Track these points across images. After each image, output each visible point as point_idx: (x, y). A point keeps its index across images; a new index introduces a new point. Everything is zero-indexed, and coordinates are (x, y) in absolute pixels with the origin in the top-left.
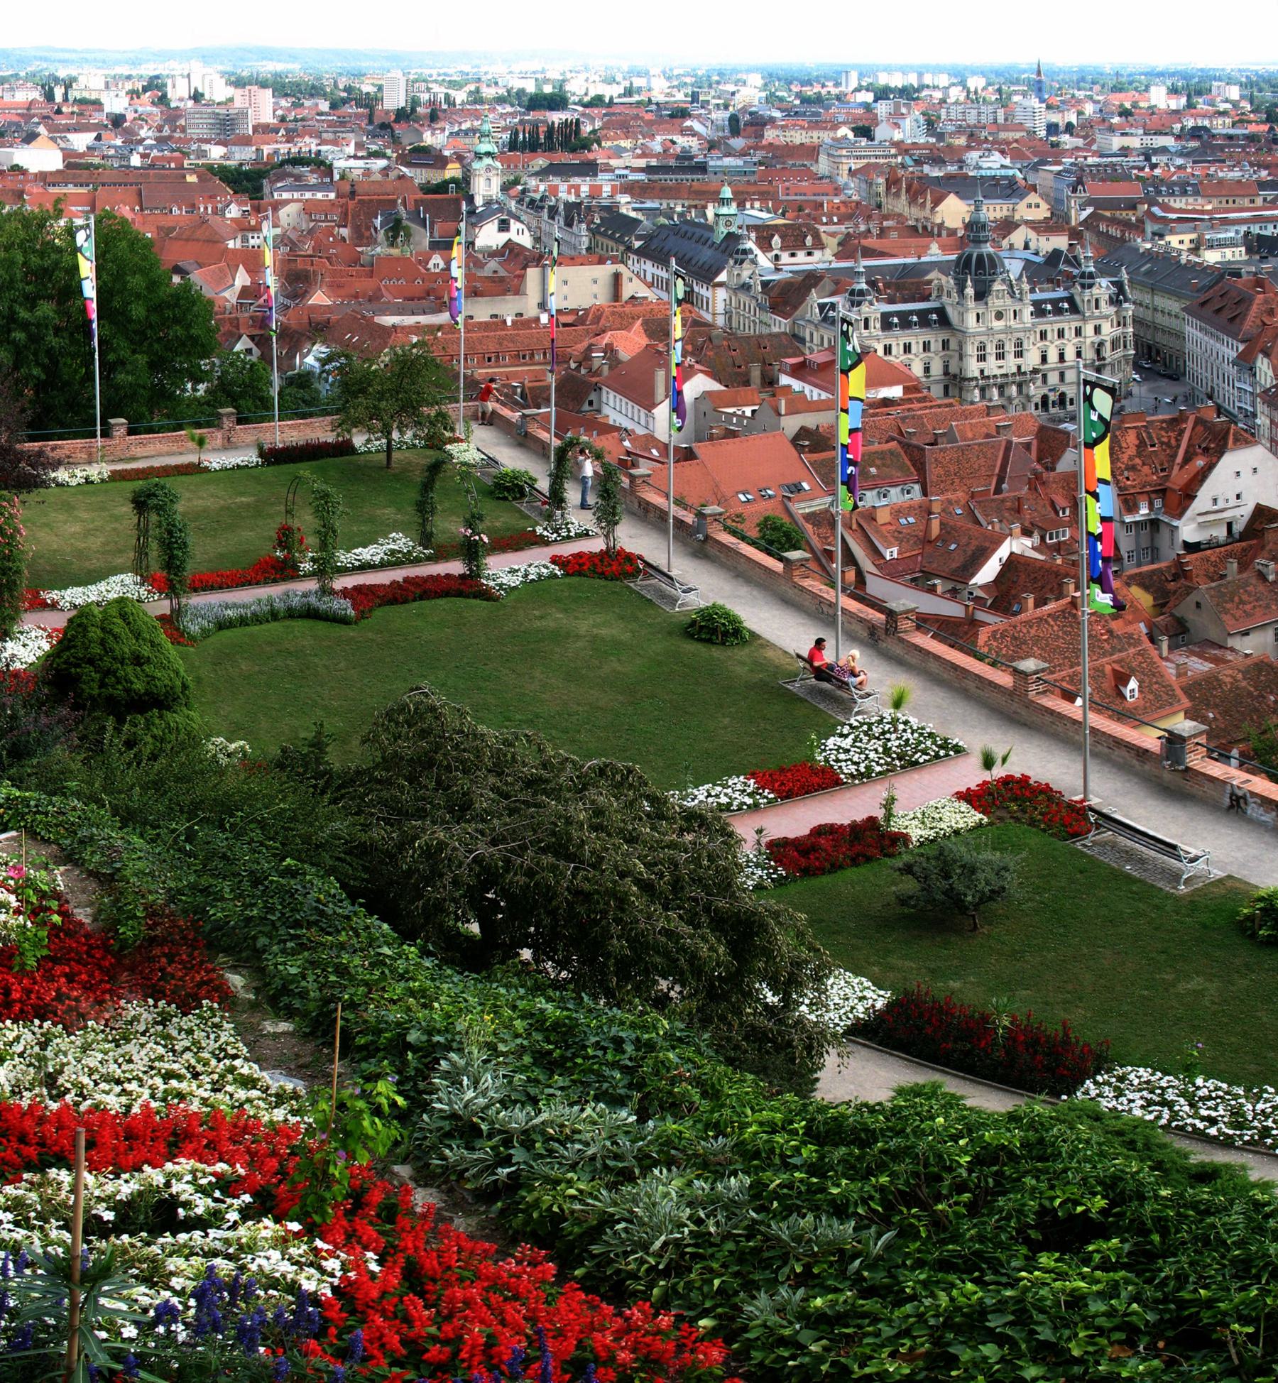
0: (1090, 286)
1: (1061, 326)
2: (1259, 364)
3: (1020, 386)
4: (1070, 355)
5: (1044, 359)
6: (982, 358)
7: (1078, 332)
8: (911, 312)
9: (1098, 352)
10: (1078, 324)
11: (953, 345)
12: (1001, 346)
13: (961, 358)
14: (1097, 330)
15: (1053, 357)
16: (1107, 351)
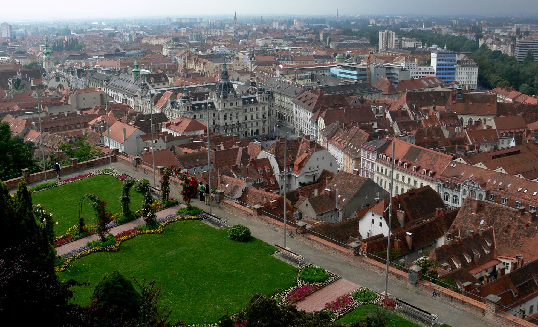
1: (251, 107)
2: (319, 120)
3: (238, 128)
4: (255, 117)
5: (246, 119)
6: (226, 119)
8: (202, 104)
9: (264, 116)
10: (257, 106)
11: (216, 115)
12: (232, 115)
13: (219, 119)
14: (263, 108)
15: (249, 118)
16: (266, 116)
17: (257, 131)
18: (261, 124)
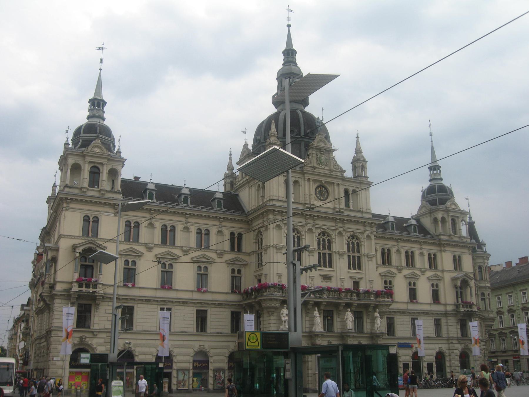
0: (443, 202)
3: (358, 318)
7: (433, 262)
11: (248, 244)
12: (325, 241)
14: (457, 262)
17: (440, 356)
18: (451, 328)
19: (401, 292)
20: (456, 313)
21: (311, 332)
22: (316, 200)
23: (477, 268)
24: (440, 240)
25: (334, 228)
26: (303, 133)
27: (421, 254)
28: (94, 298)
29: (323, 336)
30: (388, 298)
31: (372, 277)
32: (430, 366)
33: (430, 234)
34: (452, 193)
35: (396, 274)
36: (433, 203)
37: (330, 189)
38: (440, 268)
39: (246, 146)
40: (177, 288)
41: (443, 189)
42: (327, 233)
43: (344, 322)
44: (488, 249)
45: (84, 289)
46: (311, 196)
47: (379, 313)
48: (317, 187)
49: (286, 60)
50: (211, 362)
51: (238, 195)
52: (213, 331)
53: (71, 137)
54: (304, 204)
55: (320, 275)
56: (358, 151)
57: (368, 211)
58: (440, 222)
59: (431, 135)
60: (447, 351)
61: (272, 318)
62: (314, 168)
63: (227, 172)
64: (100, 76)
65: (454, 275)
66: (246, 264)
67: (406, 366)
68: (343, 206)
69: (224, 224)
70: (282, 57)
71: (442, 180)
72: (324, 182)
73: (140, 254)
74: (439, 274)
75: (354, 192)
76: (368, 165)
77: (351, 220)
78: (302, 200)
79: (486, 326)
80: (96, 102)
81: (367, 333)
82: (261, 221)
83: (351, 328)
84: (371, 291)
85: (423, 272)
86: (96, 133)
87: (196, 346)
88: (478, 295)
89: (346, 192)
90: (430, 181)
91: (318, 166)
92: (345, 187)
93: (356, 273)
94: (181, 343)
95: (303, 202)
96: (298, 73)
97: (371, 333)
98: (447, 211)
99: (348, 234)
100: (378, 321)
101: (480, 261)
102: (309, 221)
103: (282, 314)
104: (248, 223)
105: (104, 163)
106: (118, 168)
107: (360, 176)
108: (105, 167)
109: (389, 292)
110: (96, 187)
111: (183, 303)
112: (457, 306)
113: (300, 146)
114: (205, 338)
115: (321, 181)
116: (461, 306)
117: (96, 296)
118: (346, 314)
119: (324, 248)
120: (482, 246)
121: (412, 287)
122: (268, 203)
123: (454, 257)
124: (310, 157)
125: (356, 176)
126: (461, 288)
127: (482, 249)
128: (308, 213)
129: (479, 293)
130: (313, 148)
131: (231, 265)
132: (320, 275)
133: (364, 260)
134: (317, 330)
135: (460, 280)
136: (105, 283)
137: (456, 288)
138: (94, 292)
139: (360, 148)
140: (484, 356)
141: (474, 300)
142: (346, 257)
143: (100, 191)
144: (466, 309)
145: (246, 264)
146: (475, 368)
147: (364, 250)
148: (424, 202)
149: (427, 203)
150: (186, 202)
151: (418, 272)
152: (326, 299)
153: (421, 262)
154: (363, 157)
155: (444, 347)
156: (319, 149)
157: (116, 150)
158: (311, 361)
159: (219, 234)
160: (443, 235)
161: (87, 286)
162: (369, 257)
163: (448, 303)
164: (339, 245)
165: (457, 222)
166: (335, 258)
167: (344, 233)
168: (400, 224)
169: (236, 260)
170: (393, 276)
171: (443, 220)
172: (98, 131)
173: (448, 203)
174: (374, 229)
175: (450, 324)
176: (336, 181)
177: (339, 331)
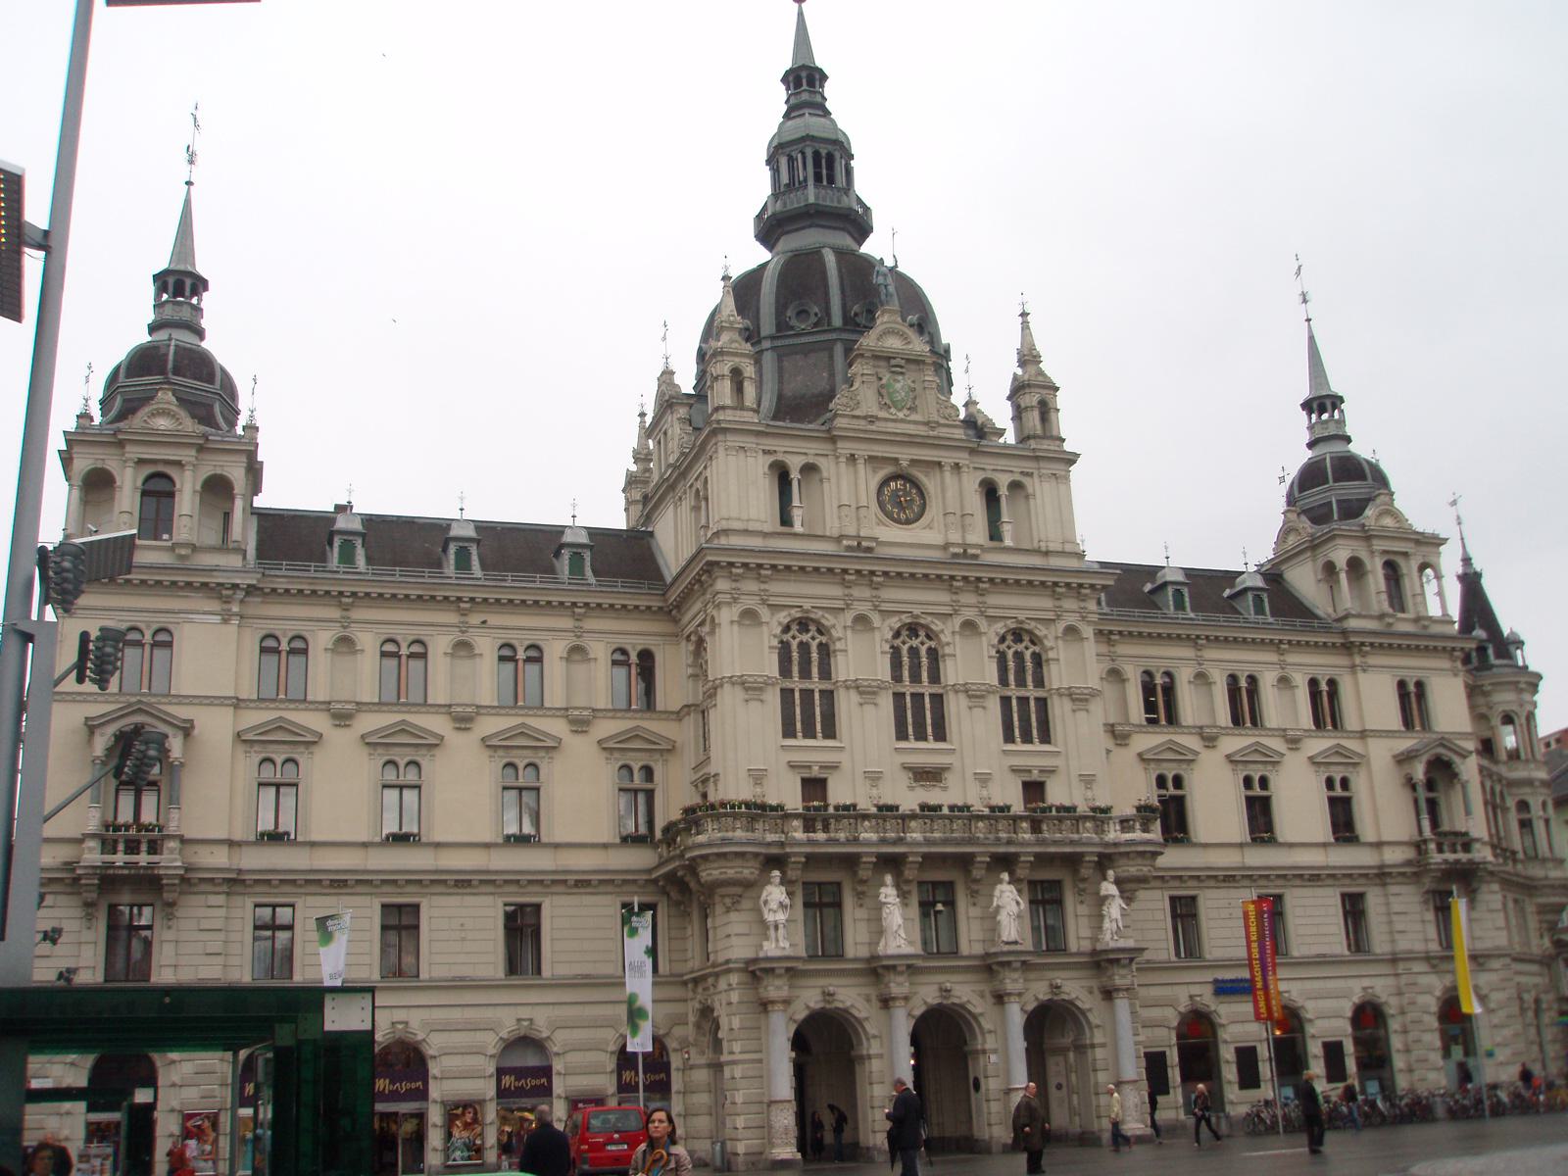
0: (1352, 510)
4: (1301, 811)
6: (809, 713)
7: (1325, 705)
11: (673, 687)
14: (1412, 701)
17: (1368, 1017)
19: (1216, 809)
20: (1416, 870)
21: (874, 958)
22: (880, 523)
23: (1496, 721)
24: (1344, 633)
25: (947, 610)
26: (837, 320)
27: (1284, 681)
28: (149, 883)
29: (912, 970)
30: (1146, 830)
31: (1097, 768)
32: (1333, 1051)
33: (1316, 617)
34: (1381, 480)
35: (1197, 753)
36: (1319, 515)
37: (930, 483)
38: (1351, 721)
39: (667, 375)
40: (439, 838)
41: (1351, 468)
42: (923, 626)
43: (991, 918)
44: (1531, 657)
45: (120, 858)
46: (863, 511)
47: (1118, 882)
48: (885, 482)
49: (793, 101)
50: (559, 1074)
51: (651, 534)
52: (563, 970)
53: (97, 391)
54: (839, 539)
55: (906, 768)
56: (1028, 357)
57: (1068, 548)
58: (1343, 576)
59: (1305, 301)
60: (1393, 1001)
61: (733, 916)
62: (872, 419)
63: (634, 468)
64: (187, 203)
65: (1406, 744)
66: (670, 750)
67: (1247, 1058)
68: (978, 535)
69: (591, 624)
70: (781, 93)
71: (1348, 440)
72: (905, 464)
73: (309, 738)
74: (1352, 745)
75: (1016, 486)
76: (1061, 400)
77: (1005, 581)
78: (832, 527)
79: (1542, 910)
80: (171, 280)
81: (1079, 954)
82: (698, 606)
83: (1014, 936)
84: (1082, 809)
85: (1294, 742)
86: (163, 372)
87: (507, 1022)
88: (1505, 810)
89: (990, 492)
90: (1311, 445)
91: (883, 414)
92: (981, 476)
93: (1032, 755)
94: (456, 1014)
95: (835, 533)
96: (833, 137)
97: (1094, 953)
98: (1367, 537)
99: (1000, 628)
100: (1114, 909)
101: (1504, 699)
102: (856, 592)
103: (766, 902)
104: (671, 613)
105: (184, 460)
106: (237, 474)
107: (1035, 437)
108: (188, 474)
109: (1171, 815)
110: (166, 536)
111: (458, 883)
112: (1419, 846)
113: (831, 357)
114: (533, 996)
115: (896, 460)
116: (1432, 846)
117: (159, 878)
118: (997, 893)
119: (916, 678)
120: (1512, 648)
121: (1257, 791)
122: (716, 543)
123: (1402, 685)
124: (856, 385)
125: (1023, 438)
126: (1430, 785)
127: (1510, 656)
128: (858, 567)
129: (1511, 803)
130: (862, 355)
131: (617, 755)
132: (906, 768)
133: (1059, 709)
134: (891, 951)
135: (1425, 758)
136: (188, 835)
137: (1414, 787)
138: (152, 866)
139: (1032, 348)
140: (1537, 1012)
141: (1478, 826)
142: (994, 705)
143: (172, 548)
144: (1450, 857)
145: (670, 750)
146: (1497, 1051)
147: (1058, 676)
148: (1293, 516)
149: (1304, 518)
150: (463, 562)
151: (1276, 744)
152: (918, 844)
153: (1285, 708)
154: (1041, 373)
155: (1381, 987)
156: (885, 358)
157: (242, 421)
158: (880, 1056)
159: (577, 657)
160: (1359, 616)
161: (132, 847)
162: (1080, 699)
163: (1385, 838)
164: (969, 663)
165: (1405, 571)
166: (955, 706)
167: (983, 625)
168: (1209, 590)
169: (635, 735)
170: (1189, 759)
171: (1355, 566)
172: (170, 365)
173: (1369, 512)
174: (1092, 606)
175: (1396, 908)
176: (947, 458)
177: (978, 949)
